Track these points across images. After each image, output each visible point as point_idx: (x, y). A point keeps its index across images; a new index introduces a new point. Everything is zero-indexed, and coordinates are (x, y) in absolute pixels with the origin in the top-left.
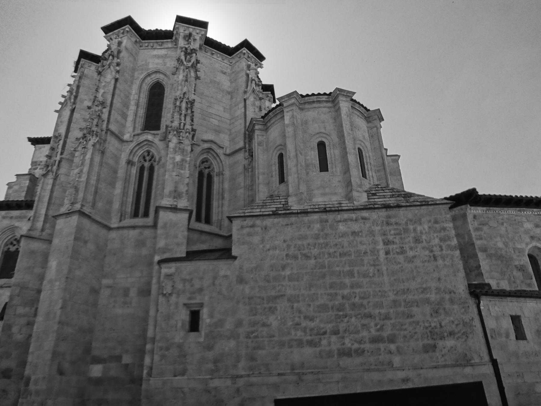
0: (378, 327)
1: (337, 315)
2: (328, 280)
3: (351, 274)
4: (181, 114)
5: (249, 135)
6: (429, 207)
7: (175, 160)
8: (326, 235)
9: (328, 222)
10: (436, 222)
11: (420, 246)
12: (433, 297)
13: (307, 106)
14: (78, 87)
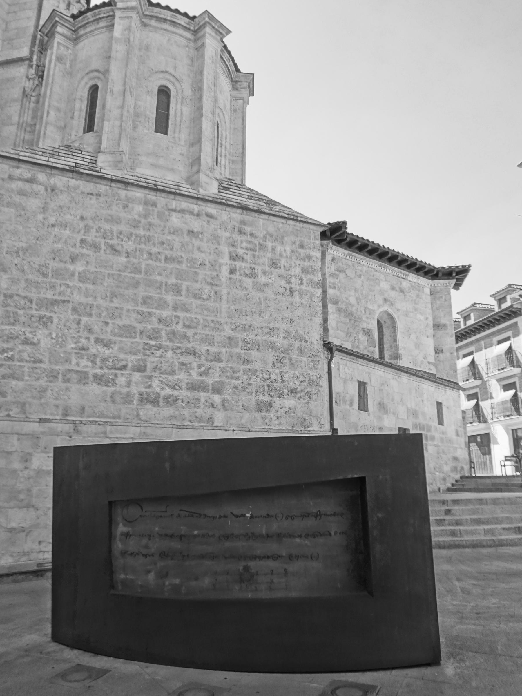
0: (203, 369)
1: (146, 344)
2: (142, 292)
3: (177, 290)
5: (41, 41)
6: (297, 224)
8: (150, 224)
9: (156, 206)
10: (302, 246)
11: (276, 272)
12: (280, 341)
13: (153, 22)
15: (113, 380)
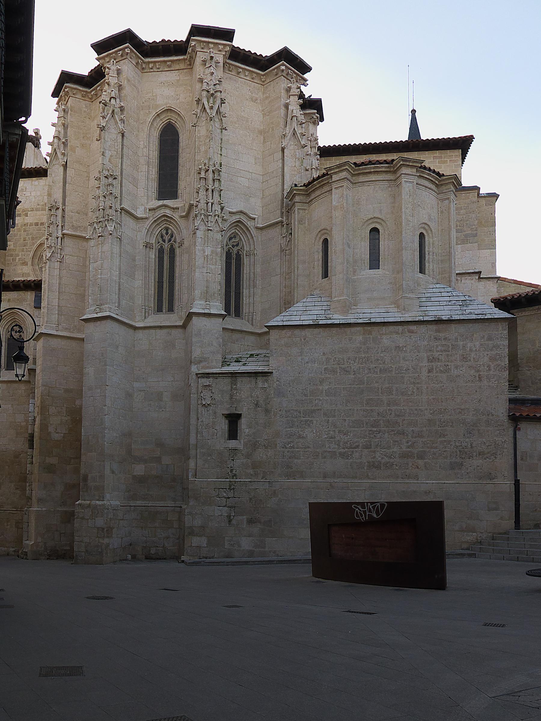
4: (207, 190)
7: (204, 252)
14: (65, 126)
15: (351, 455)
